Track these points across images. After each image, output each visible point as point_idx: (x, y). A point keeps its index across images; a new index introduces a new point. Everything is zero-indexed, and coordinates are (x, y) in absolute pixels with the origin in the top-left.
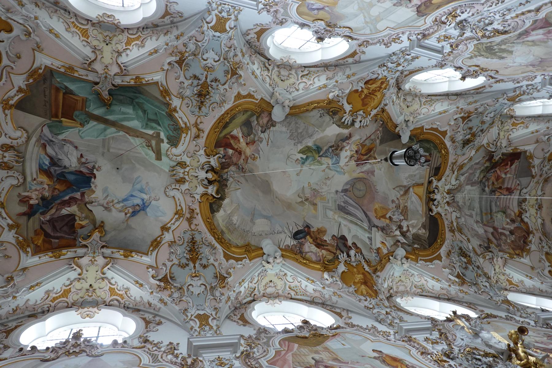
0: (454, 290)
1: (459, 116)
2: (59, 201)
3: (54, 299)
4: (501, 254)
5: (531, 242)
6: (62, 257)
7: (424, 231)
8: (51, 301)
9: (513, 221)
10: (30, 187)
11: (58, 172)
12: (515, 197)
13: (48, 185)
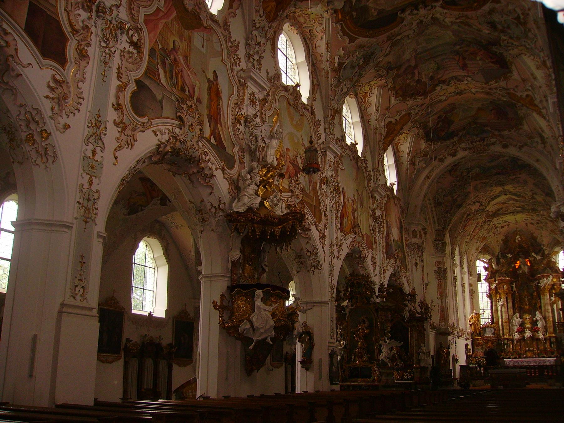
0: (325, 66)
1: (520, 12)
4: (391, 80)
5: (416, 99)
7: (376, 14)
9: (432, 78)
12: (461, 73)
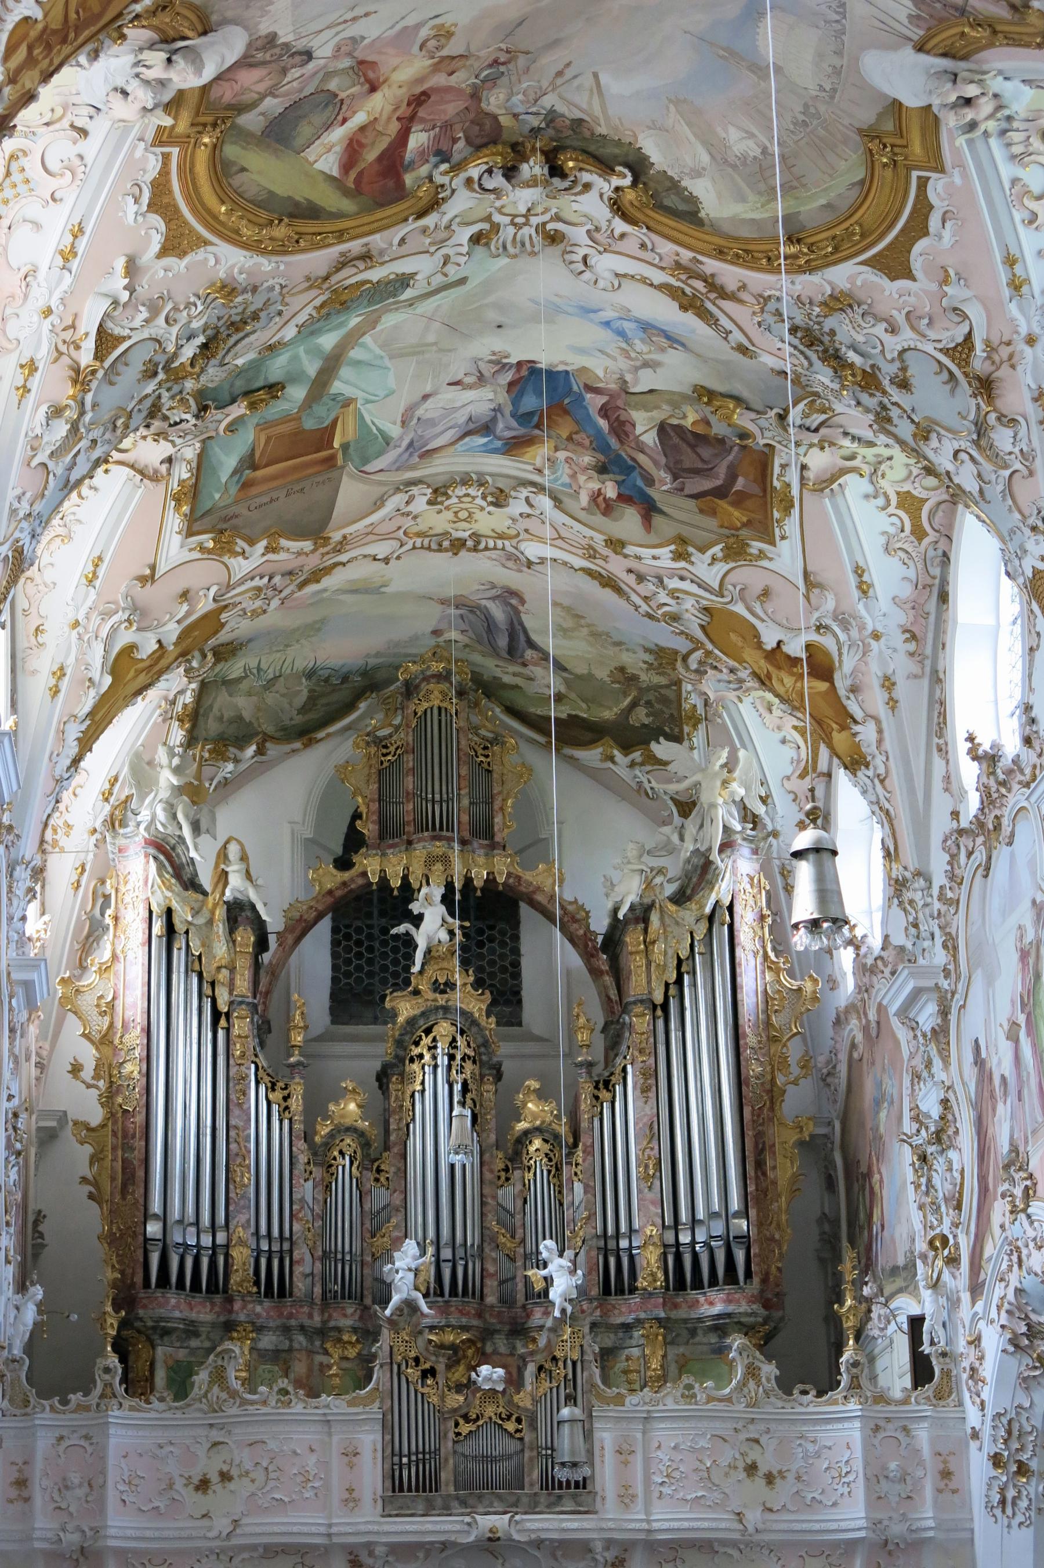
2: (613, 442)
3: (919, 533)
6: (795, 491)
8: (920, 540)
10: (563, 485)
11: (514, 424)
13: (556, 449)
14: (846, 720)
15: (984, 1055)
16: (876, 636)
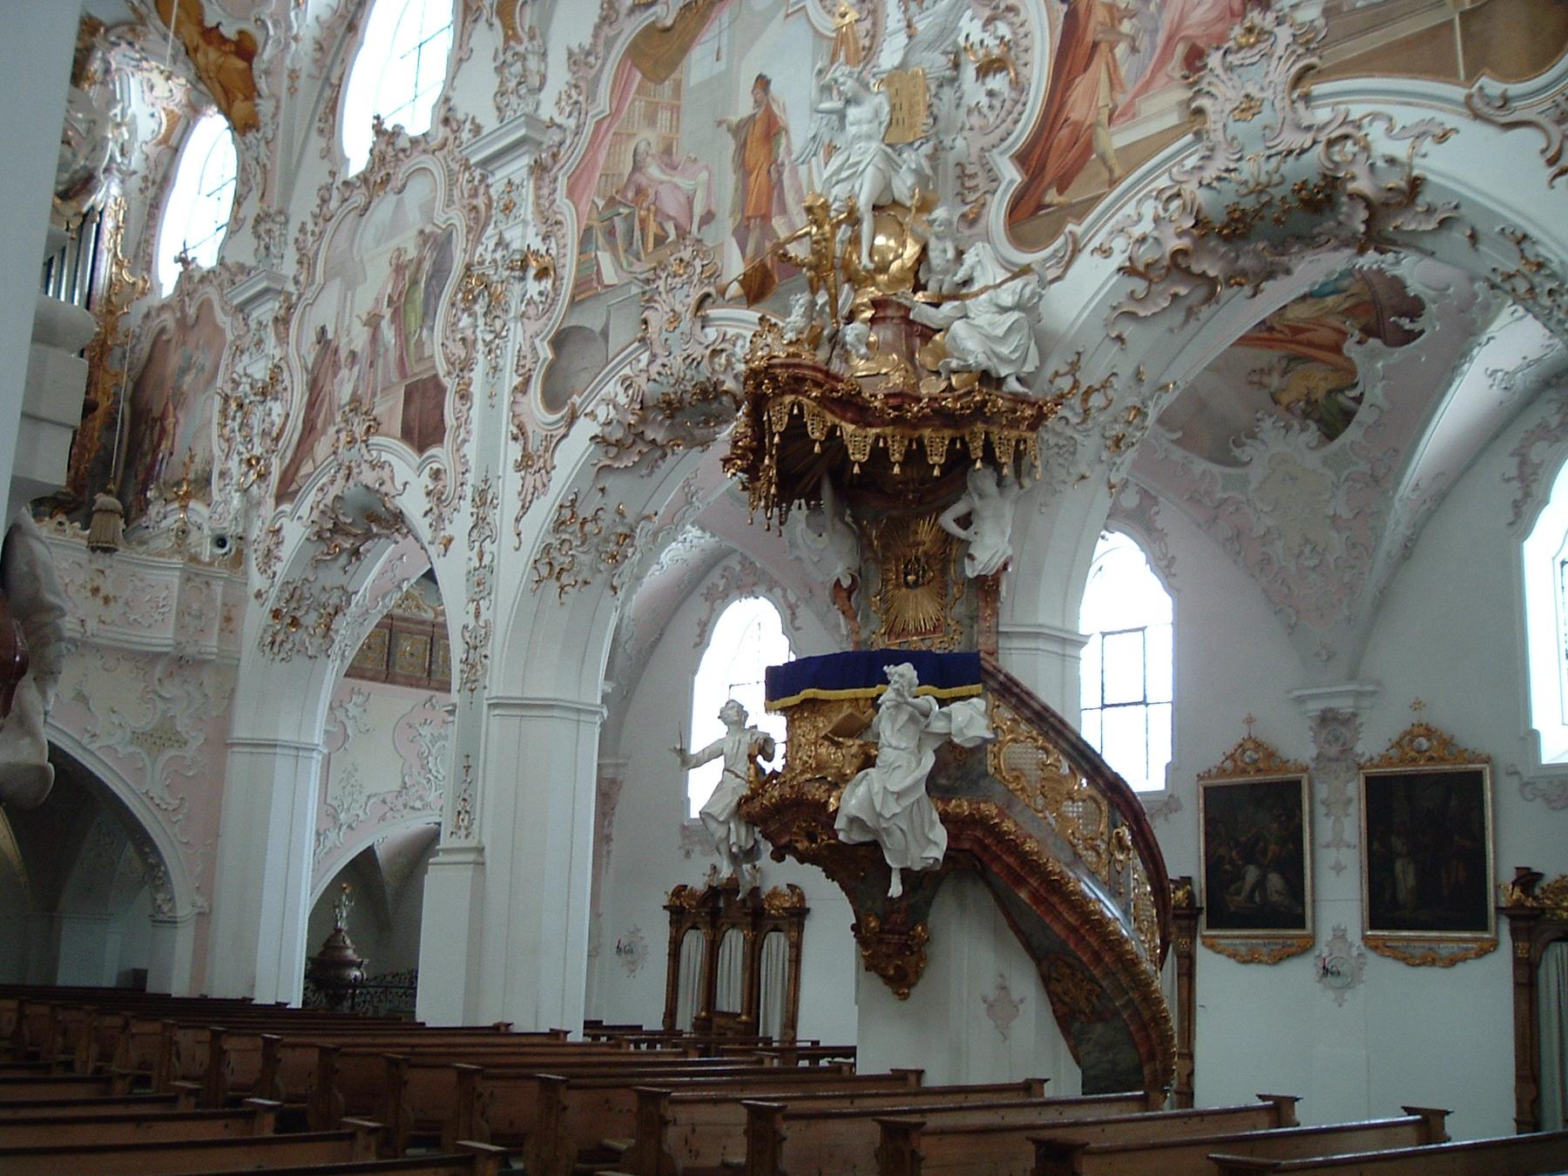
14: (251, 92)
15: (330, 336)
16: (296, 39)
